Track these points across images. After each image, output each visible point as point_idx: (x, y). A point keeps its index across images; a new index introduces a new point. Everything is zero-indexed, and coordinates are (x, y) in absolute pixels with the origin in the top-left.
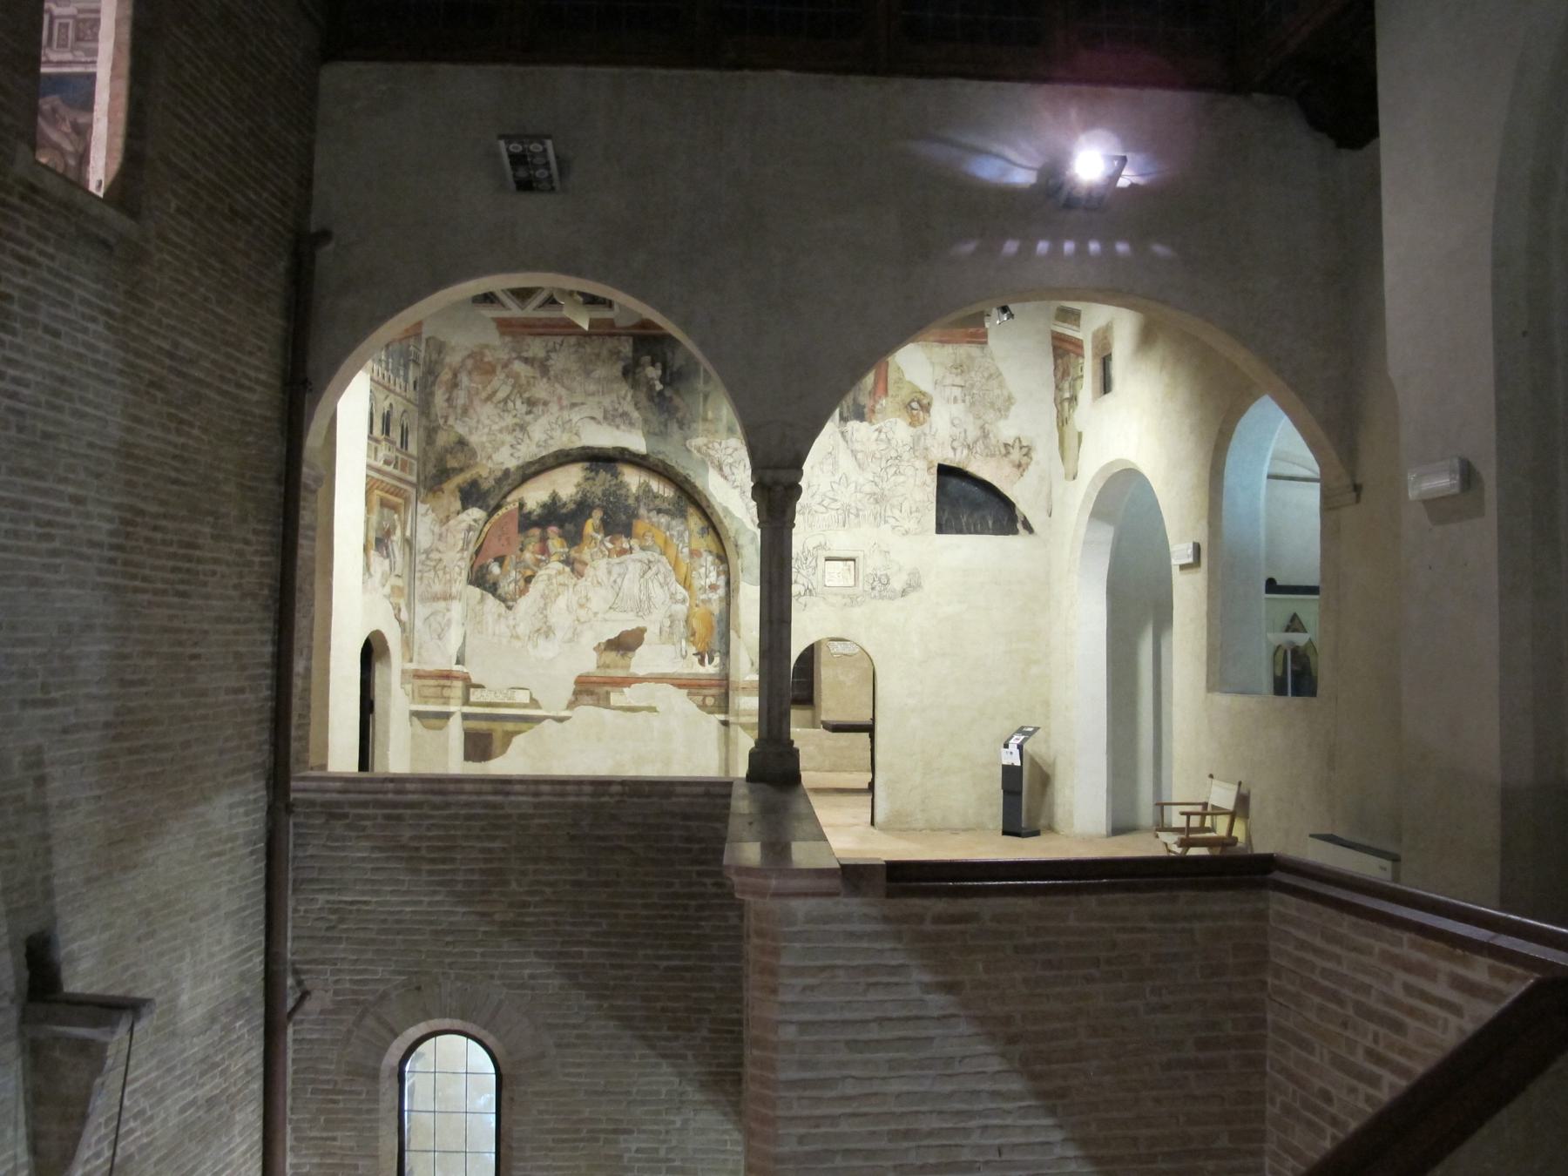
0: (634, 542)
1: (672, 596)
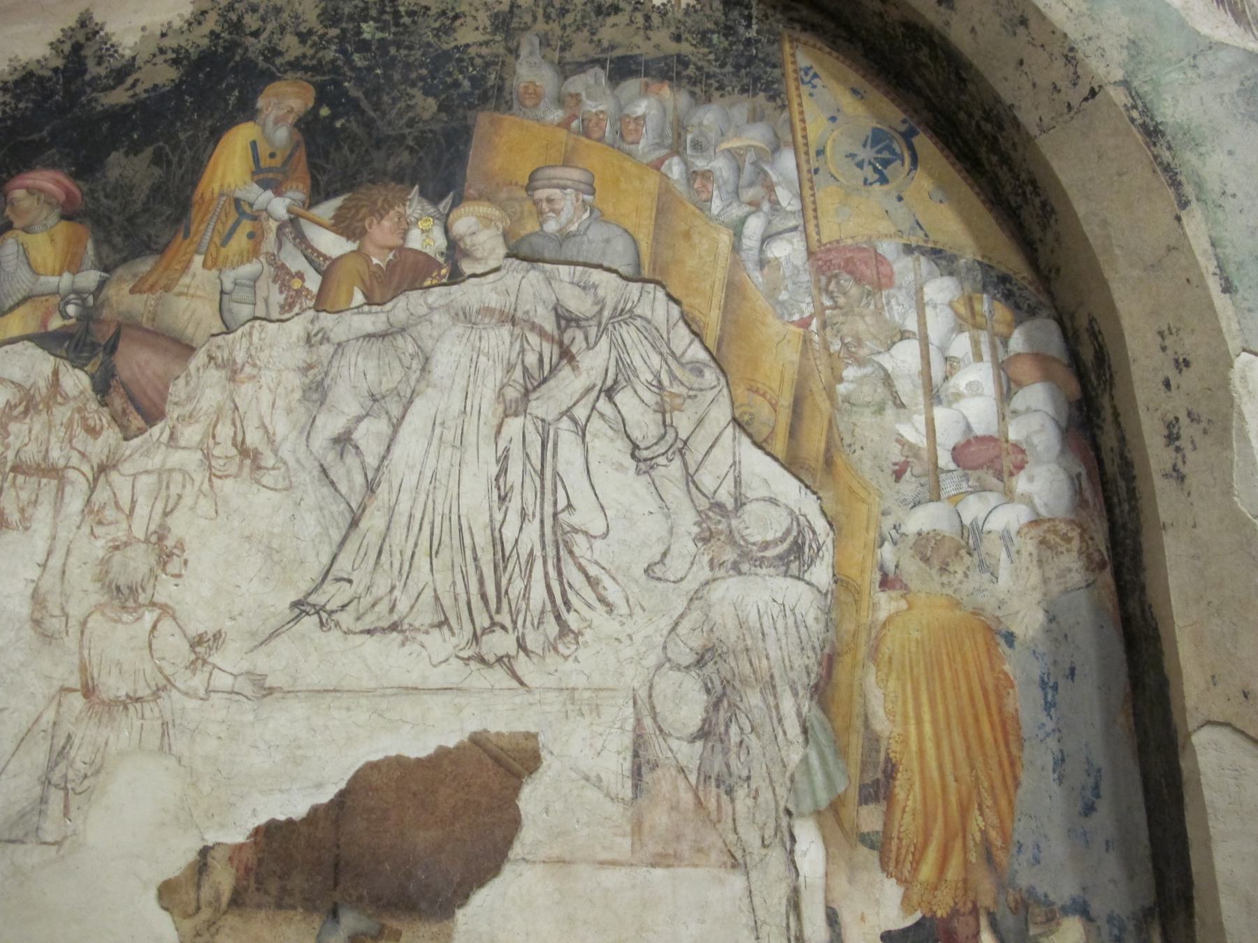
0: (476, 225)
1: (717, 520)
